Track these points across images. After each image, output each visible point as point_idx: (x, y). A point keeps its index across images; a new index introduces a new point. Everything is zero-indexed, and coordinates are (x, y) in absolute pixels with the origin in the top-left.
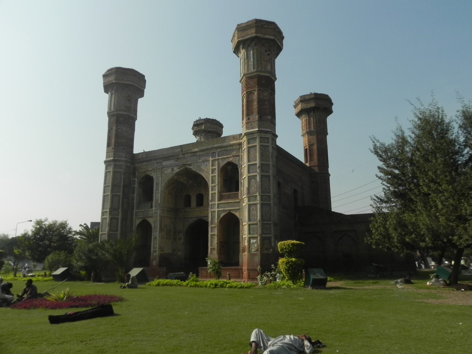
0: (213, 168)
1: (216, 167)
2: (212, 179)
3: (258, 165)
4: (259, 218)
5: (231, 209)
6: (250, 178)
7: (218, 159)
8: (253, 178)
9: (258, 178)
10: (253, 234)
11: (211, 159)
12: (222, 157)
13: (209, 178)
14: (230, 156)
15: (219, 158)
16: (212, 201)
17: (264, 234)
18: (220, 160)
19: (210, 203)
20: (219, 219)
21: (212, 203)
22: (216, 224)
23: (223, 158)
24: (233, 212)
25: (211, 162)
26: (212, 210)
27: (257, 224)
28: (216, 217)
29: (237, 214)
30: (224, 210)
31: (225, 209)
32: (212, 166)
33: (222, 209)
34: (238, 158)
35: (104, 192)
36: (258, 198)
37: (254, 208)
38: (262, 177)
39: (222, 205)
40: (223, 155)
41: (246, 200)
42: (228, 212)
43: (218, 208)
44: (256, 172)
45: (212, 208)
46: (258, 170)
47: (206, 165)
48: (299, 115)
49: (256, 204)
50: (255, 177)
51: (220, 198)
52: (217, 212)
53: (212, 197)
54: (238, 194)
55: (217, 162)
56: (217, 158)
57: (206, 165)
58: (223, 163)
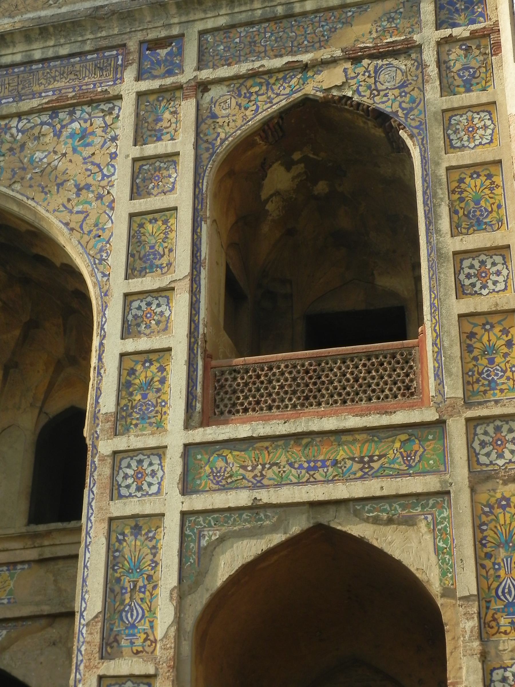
0: (151, 149)
1: (184, 144)
2: (135, 238)
5: (341, 491)
7: (203, 87)
11: (129, 86)
12: (244, 68)
13: (96, 237)
14: (325, 54)
15: (205, 74)
16: (121, 422)
18: (215, 92)
19: (105, 446)
20: (199, 601)
21: (121, 443)
22: (164, 652)
23: (253, 75)
24: (357, 529)
25: (127, 108)
26: (119, 508)
28: (168, 577)
29: (412, 549)
30: (256, 508)
31: (266, 496)
32: (138, 139)
33: (241, 498)
34: (402, 63)
39: (232, 462)
40: (252, 50)
42: (297, 527)
43: (187, 489)
45: (115, 492)
47: (84, 135)
51: (214, 399)
52: (172, 525)
53: (124, 386)
54: (408, 361)
55: (187, 108)
56: (188, 73)
57: (84, 135)
58: (239, 117)
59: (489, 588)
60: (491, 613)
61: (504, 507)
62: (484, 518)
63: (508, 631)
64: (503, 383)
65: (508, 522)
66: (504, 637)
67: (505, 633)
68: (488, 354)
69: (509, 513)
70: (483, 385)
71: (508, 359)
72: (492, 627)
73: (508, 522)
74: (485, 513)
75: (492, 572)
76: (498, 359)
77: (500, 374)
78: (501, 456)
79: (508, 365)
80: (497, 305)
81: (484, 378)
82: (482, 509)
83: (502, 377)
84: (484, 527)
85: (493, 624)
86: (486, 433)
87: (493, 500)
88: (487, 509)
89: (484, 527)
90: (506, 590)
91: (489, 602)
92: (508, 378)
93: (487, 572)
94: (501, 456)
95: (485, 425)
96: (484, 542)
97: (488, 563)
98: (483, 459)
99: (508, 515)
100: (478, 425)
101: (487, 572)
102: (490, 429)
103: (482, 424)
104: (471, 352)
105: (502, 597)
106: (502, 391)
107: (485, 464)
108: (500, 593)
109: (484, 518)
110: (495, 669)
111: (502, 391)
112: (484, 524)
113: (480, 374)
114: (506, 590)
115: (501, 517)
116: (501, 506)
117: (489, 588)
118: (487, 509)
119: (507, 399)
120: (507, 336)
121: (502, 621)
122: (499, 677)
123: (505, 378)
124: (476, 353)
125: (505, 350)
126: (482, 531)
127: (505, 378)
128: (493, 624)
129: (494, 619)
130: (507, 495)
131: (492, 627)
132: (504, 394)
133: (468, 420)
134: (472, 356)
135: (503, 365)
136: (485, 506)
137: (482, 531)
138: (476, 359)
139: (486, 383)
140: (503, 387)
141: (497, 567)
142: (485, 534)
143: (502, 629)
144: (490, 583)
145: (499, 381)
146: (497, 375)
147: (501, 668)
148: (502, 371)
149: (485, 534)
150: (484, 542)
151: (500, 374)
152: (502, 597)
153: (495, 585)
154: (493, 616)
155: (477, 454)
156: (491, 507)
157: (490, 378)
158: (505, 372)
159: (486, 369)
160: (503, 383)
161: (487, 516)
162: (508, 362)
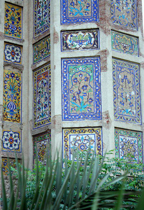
37: (130, 77)
59: (6, 104)
60: (5, 112)
61: (12, 77)
62: (6, 79)
63: (10, 120)
64: (16, 33)
65: (13, 82)
66: (8, 121)
67: (9, 120)
68: (12, 20)
69: (14, 79)
70: (9, 31)
71: (18, 24)
72: (5, 117)
73: (13, 82)
74: (6, 77)
75: (7, 98)
76: (15, 23)
77: (16, 29)
78: (13, 58)
79: (18, 27)
80: (18, 3)
81: (10, 28)
82: (6, 76)
83: (16, 30)
84: (6, 82)
85: (6, 116)
86: (9, 49)
87: (9, 74)
88: (7, 76)
89: (6, 82)
90: (11, 106)
91: (5, 108)
92: (18, 31)
93: (5, 98)
94: (13, 58)
95: (9, 46)
96: (5, 87)
97: (6, 95)
98: (7, 58)
99: (13, 80)
100: (7, 45)
101: (5, 98)
102: (11, 48)
103: (8, 45)
104: (7, 17)
105: (9, 108)
106: (15, 35)
107: (8, 60)
108: (9, 107)
109: (6, 79)
110: (5, 132)
111: (15, 35)
112: (6, 81)
113: (9, 26)
114: (11, 106)
115: (11, 80)
116: (11, 76)
117: (6, 104)
118: (7, 76)
119: (17, 39)
120: (19, 16)
121: (9, 116)
122: (6, 135)
123: (17, 31)
124: (9, 18)
125: (17, 20)
126: (5, 83)
127: (17, 31)
128: (6, 116)
129: (6, 115)
130: (14, 73)
131: (5, 117)
132: (16, 37)
133: (5, 42)
134: (7, 18)
135: (16, 26)
136: (7, 75)
137: (5, 83)
138: (8, 20)
139: (11, 30)
140: (16, 34)
141: (9, 97)
142: (6, 84)
143: (8, 119)
144: (6, 102)
145: (15, 31)
146: (14, 29)
147: (7, 131)
148: (16, 28)
149: (6, 84)
150: (5, 87)
151: (16, 29)
152: (9, 108)
153: (7, 103)
154: (6, 114)
155: (6, 55)
156: (9, 76)
157: (12, 29)
158: (17, 28)
159: (11, 25)
160: (16, 33)
161: (7, 78)
162: (18, 25)
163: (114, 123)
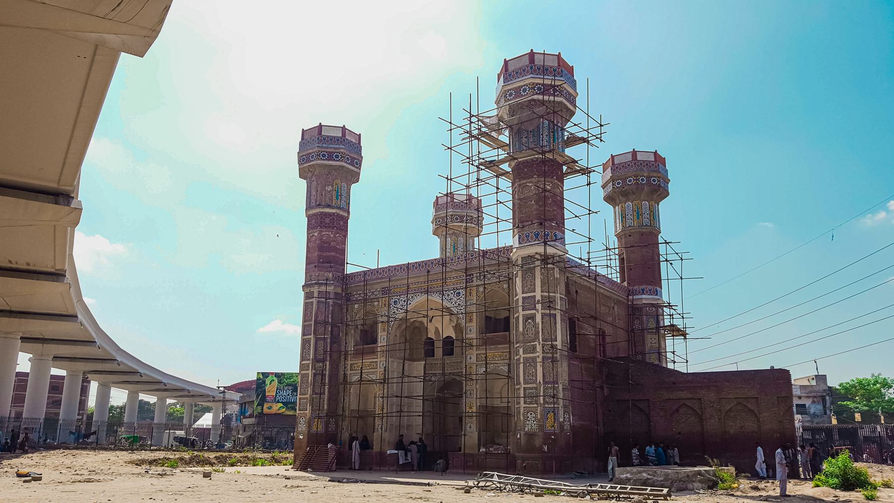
3: (538, 297)
4: (540, 378)
6: (527, 318)
8: (530, 318)
9: (539, 319)
10: (531, 403)
17: (548, 403)
27: (536, 388)
35: (304, 334)
36: (539, 348)
38: (543, 315)
41: (521, 350)
44: (535, 308)
46: (539, 306)
48: (609, 199)
49: (534, 360)
50: (533, 317)
163: (524, 386)
